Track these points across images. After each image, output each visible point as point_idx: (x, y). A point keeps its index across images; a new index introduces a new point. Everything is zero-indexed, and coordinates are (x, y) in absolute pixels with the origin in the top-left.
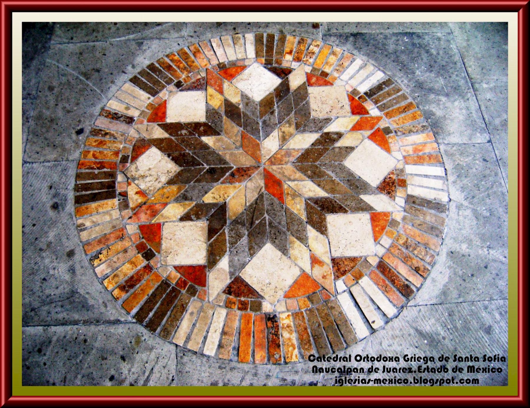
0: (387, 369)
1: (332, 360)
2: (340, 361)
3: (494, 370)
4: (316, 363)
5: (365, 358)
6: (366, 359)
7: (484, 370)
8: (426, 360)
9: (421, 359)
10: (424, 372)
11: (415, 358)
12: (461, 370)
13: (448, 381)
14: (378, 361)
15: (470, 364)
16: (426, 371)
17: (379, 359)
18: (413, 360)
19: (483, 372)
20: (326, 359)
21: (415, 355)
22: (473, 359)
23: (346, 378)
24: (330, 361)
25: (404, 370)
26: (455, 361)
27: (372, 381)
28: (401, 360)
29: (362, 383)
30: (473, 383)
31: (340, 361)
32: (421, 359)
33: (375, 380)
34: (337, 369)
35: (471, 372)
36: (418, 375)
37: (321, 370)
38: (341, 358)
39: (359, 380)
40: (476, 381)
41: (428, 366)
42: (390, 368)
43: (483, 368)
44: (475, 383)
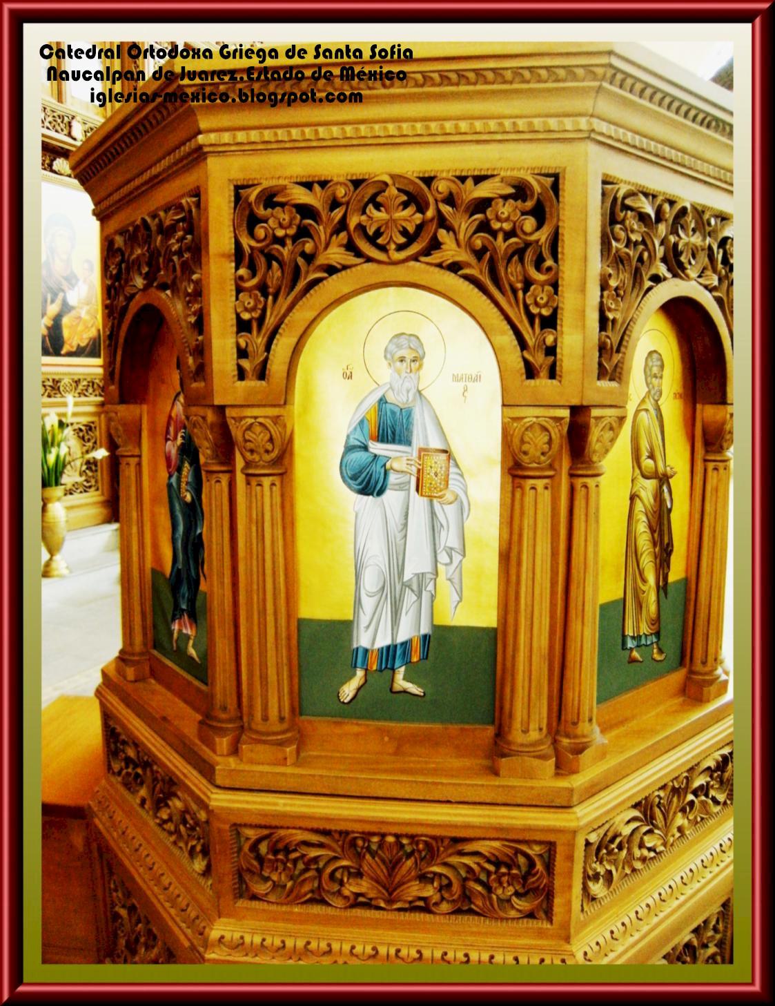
0: (189, 72)
1: (84, 56)
6: (148, 54)
11: (241, 50)
18: (238, 54)
21: (241, 45)
24: (80, 58)
26: (317, 57)
31: (100, 57)
34: (93, 73)
38: (101, 51)
39: (135, 94)
44: (356, 101)
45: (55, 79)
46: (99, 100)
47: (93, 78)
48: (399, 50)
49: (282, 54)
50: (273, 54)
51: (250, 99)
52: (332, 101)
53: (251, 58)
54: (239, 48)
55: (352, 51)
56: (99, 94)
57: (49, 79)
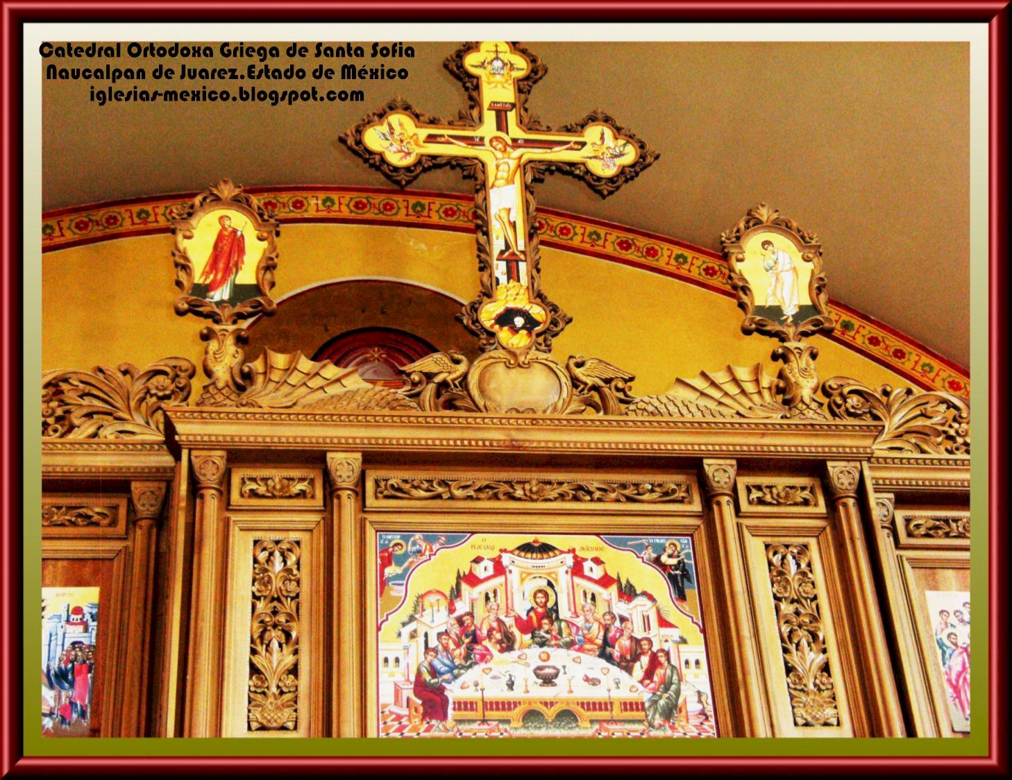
0: (189, 70)
1: (83, 54)
2: (100, 55)
4: (53, 59)
5: (146, 49)
6: (148, 52)
7: (374, 74)
9: (254, 51)
10: (259, 77)
12: (329, 73)
13: (305, 96)
14: (173, 56)
15: (348, 61)
16: (263, 74)
20: (72, 52)
23: (110, 89)
24: (80, 56)
25: (221, 73)
26: (318, 55)
27: (161, 95)
28: (217, 52)
29: (143, 99)
30: (352, 99)
31: (100, 55)
33: (167, 92)
35: (349, 78)
36: (247, 84)
37: (64, 74)
38: (101, 49)
39: (135, 92)
40: (358, 95)
41: (266, 66)
43: (371, 70)
44: (357, 99)
45: (55, 77)
46: (99, 98)
47: (93, 76)
48: (401, 48)
49: (283, 52)
51: (250, 98)
52: (332, 99)
53: (251, 56)
54: (239, 46)
55: (353, 49)
56: (99, 93)
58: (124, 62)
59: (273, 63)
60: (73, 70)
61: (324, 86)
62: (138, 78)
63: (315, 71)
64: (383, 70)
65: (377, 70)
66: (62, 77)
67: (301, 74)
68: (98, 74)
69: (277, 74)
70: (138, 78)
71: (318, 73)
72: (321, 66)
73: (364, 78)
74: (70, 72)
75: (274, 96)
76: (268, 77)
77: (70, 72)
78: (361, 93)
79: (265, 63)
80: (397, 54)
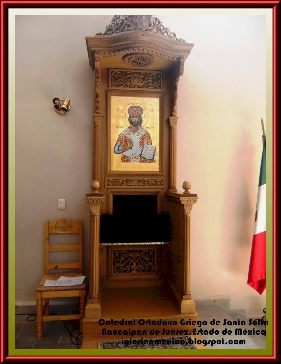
0: (166, 331)
1: (119, 324)
2: (126, 324)
3: (258, 332)
4: (105, 326)
5: (147, 322)
6: (148, 323)
8: (199, 323)
10: (198, 334)
11: (190, 322)
12: (230, 332)
15: (238, 327)
16: (200, 333)
17: (159, 323)
18: (189, 323)
19: (249, 334)
21: (190, 319)
22: (240, 323)
24: (117, 325)
25: (181, 332)
26: (224, 324)
30: (240, 344)
31: (126, 324)
32: (195, 322)
34: (123, 331)
35: (239, 334)
37: (110, 333)
38: (126, 322)
40: (243, 342)
41: (201, 329)
42: (169, 331)
43: (249, 331)
44: (242, 344)
45: (106, 334)
49: (209, 323)
50: (205, 323)
51: (194, 343)
52: (232, 343)
53: (194, 325)
54: (189, 320)
55: (241, 322)
57: (103, 334)
58: (137, 327)
59: (204, 328)
60: (114, 331)
61: (227, 338)
62: (143, 334)
63: (223, 331)
64: (254, 331)
65: (251, 331)
66: (109, 334)
67: (217, 332)
68: (125, 333)
69: (206, 333)
70: (143, 334)
71: (224, 333)
72: (226, 329)
73: (245, 334)
74: (112, 332)
75: (205, 342)
76: (202, 334)
77: (112, 332)
78: (244, 341)
79: (201, 328)
80: (260, 324)
